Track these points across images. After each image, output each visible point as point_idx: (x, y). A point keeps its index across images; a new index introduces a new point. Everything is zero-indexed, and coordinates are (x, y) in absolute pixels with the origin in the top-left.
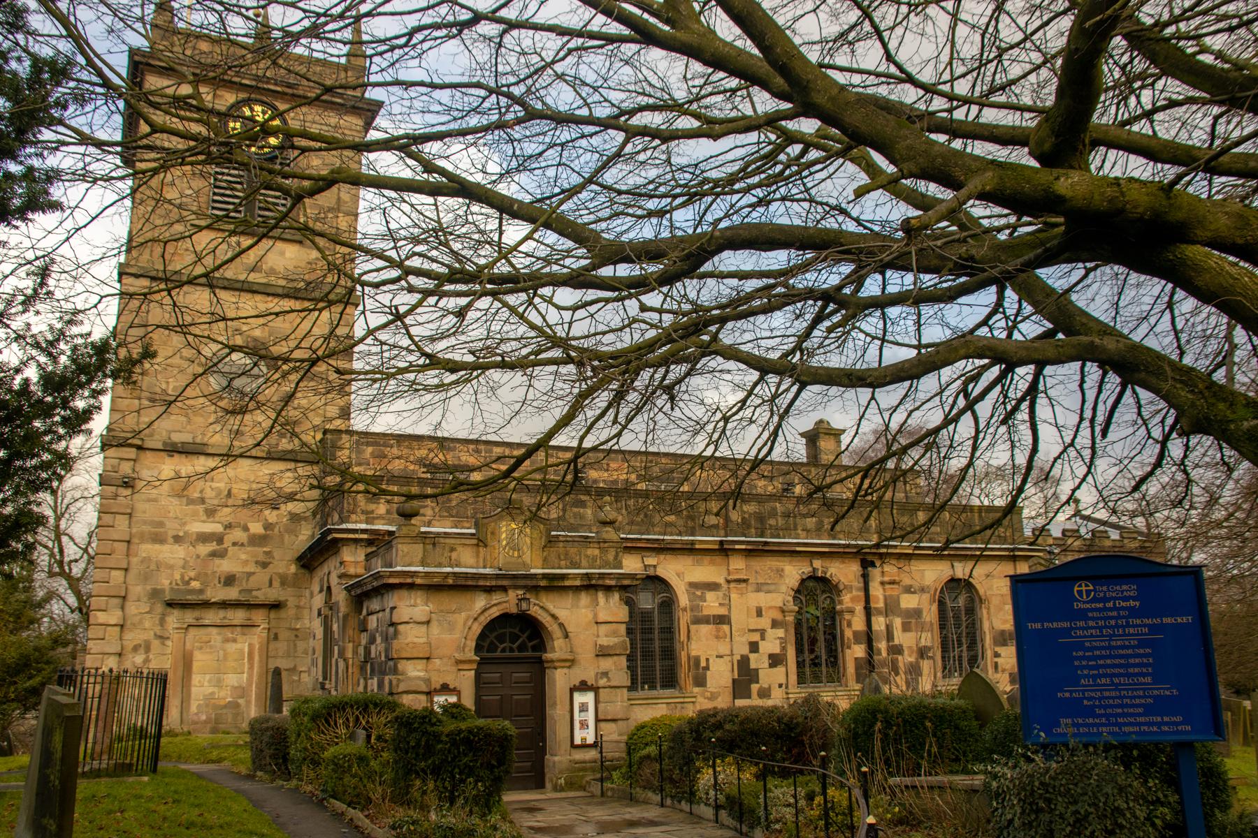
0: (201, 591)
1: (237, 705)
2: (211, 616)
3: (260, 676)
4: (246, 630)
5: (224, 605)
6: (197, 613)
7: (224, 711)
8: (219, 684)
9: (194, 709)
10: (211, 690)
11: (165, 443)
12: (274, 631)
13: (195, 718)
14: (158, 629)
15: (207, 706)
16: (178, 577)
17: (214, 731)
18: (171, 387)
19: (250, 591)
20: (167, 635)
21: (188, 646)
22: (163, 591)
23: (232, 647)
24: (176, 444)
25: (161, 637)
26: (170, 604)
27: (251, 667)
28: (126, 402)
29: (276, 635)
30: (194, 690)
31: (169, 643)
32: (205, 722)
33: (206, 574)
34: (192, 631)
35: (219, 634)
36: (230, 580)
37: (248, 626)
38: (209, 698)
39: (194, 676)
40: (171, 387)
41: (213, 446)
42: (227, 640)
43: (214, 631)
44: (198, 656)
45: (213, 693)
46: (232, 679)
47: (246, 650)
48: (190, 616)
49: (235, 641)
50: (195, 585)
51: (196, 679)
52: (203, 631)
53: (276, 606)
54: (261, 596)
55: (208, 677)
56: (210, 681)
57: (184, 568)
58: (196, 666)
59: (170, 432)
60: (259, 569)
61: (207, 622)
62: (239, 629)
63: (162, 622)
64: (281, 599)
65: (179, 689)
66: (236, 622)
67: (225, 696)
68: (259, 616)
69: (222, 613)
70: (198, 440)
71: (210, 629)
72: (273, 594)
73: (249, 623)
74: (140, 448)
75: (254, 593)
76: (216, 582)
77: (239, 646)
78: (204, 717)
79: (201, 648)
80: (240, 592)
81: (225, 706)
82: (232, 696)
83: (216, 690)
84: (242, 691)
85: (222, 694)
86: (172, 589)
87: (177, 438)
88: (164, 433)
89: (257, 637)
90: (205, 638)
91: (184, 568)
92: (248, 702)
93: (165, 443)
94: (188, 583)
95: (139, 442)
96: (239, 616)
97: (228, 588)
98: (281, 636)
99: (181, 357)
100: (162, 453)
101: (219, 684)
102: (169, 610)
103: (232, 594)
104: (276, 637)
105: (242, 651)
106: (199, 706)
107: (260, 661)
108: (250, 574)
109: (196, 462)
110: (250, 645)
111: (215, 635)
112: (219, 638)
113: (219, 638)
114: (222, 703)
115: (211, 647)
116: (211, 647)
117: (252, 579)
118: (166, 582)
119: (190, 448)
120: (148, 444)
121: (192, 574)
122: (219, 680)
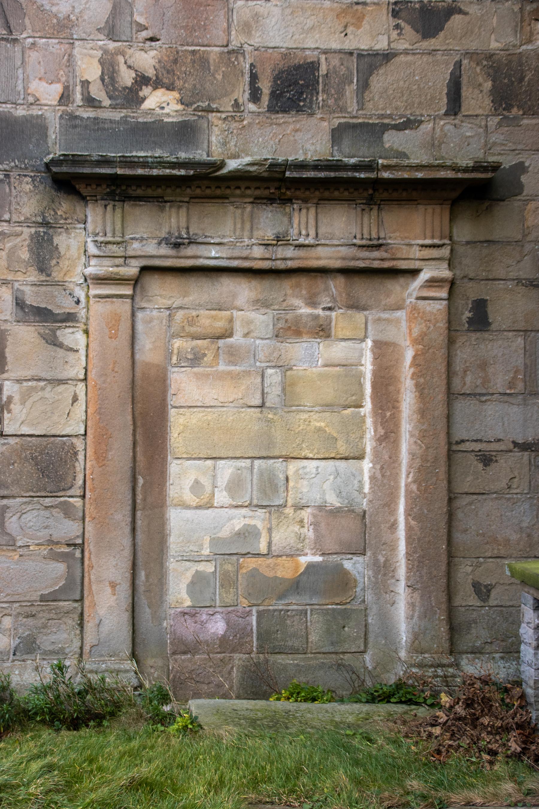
0: (185, 132)
1: (342, 582)
2: (231, 234)
3: (423, 472)
4: (363, 289)
5: (279, 186)
6: (174, 221)
7: (294, 603)
8: (270, 498)
9: (179, 591)
10: (239, 520)
12: (473, 291)
13: (188, 630)
14: (27, 281)
15: (228, 581)
16: (90, 70)
17: (259, 684)
19: (374, 131)
20: (66, 305)
21: (148, 351)
22: (37, 127)
23: (310, 357)
25: (42, 314)
26: (70, 182)
27: (388, 435)
29: (480, 308)
30: (176, 518)
31: (73, 337)
32: (225, 644)
33: (202, 62)
34: (163, 294)
35: (262, 304)
36: (293, 86)
37: (372, 274)
38: (235, 551)
39: (174, 468)
42: (290, 329)
43: (244, 291)
44: (185, 386)
45: (247, 534)
46: (317, 482)
47: (368, 368)
48: (146, 233)
49: (323, 331)
50: (161, 103)
51: (183, 477)
52: (200, 292)
53: (472, 193)
54: (411, 151)
55: (226, 470)
56: (235, 486)
57: (111, 31)
58: (181, 427)
60: (406, 40)
61: (212, 255)
62: (335, 286)
63: (44, 254)
64: (507, 161)
65: (122, 516)
66: (325, 256)
67: (294, 544)
68: (411, 235)
69: (269, 222)
71: (228, 286)
72: (460, 143)
73: (373, 259)
75: (391, 139)
76: (242, 93)
77: (338, 351)
78: (218, 627)
79: (196, 359)
80: (337, 134)
81: (296, 586)
82: (319, 547)
83: (258, 520)
84: (359, 529)
85: (284, 536)
86: (71, 121)
89: (408, 317)
90: (209, 321)
91: (111, 31)
92: (383, 571)
94: (131, 97)
96: (332, 233)
97: (289, 122)
98: (499, 315)
101: (270, 498)
102: (65, 206)
103: (306, 140)
104: (480, 320)
105: (349, 368)
106: (198, 582)
107: (423, 412)
108: (372, 62)
110: (384, 351)
111: (246, 309)
112: (262, 320)
113: (262, 320)
114: (285, 570)
115: (233, 355)
116: (233, 355)
117: (379, 81)
118: (48, 93)
121: (147, 60)
122: (270, 485)
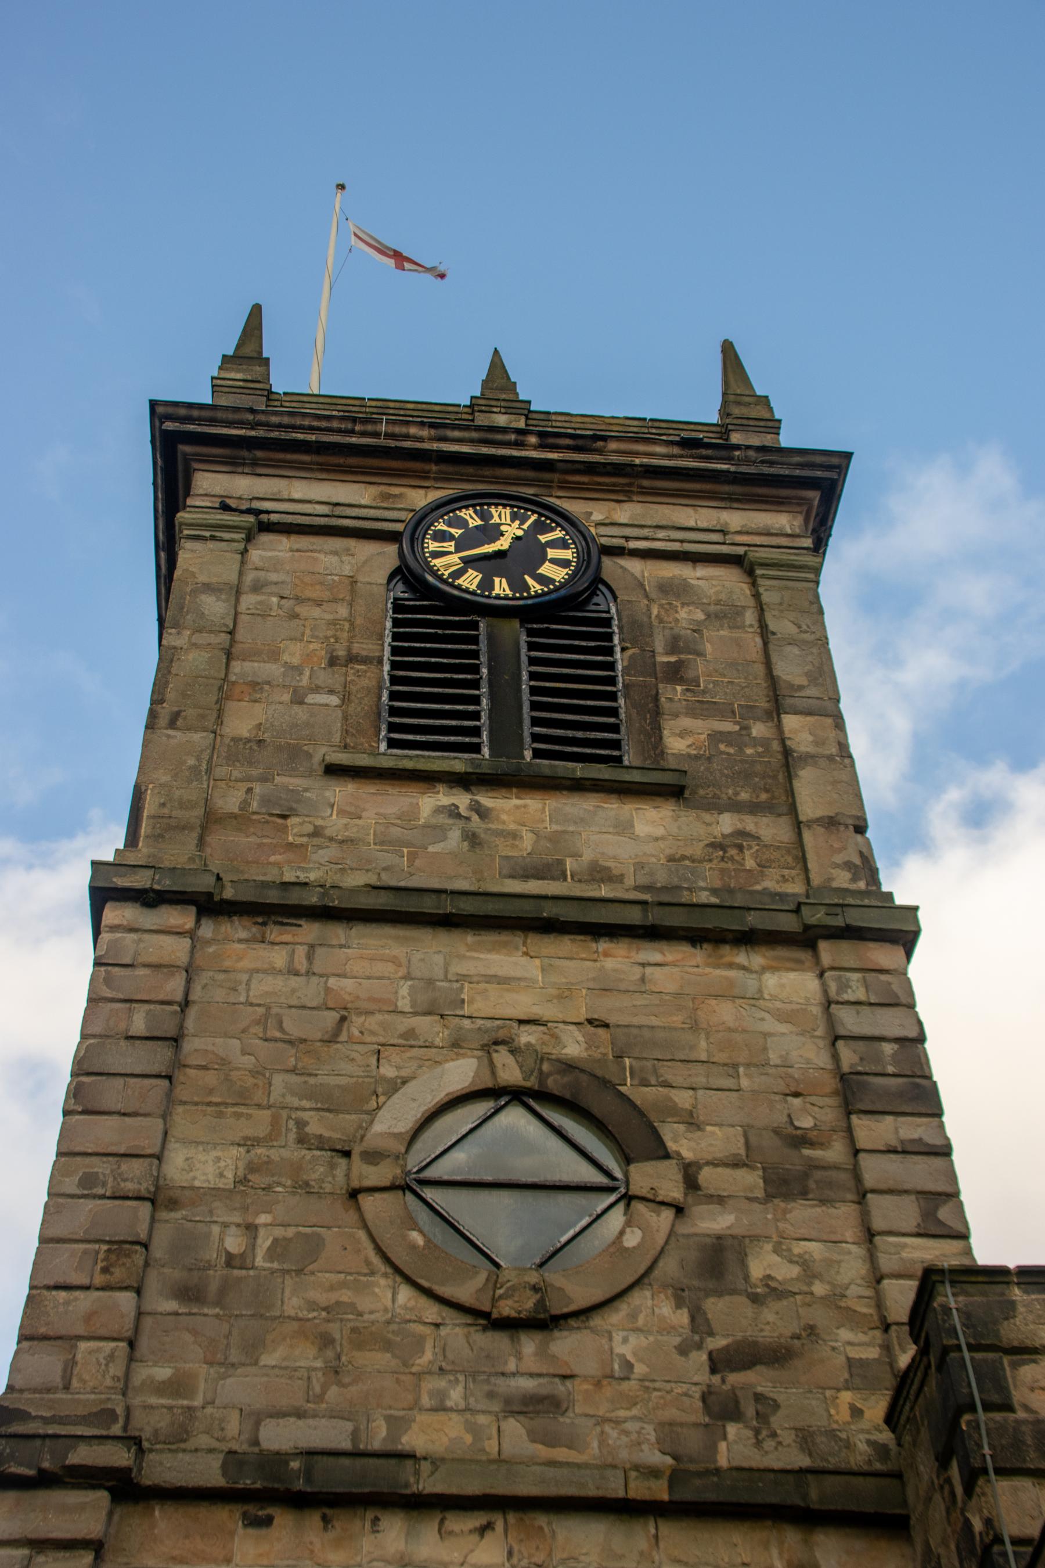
11: (233, 1460)
18: (264, 1243)
24: (278, 1459)
28: (85, 1301)
40: (264, 1243)
41: (436, 1462)
59: (257, 1418)
70: (378, 1437)
74: (127, 1490)
87: (280, 1436)
88: (233, 1426)
93: (233, 1460)
95: (120, 1457)
99: (302, 1140)
100: (226, 1516)
109: (367, 1543)
119: (339, 1477)
120: (165, 1468)
